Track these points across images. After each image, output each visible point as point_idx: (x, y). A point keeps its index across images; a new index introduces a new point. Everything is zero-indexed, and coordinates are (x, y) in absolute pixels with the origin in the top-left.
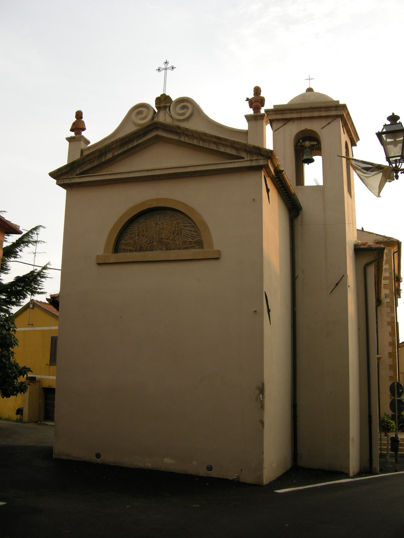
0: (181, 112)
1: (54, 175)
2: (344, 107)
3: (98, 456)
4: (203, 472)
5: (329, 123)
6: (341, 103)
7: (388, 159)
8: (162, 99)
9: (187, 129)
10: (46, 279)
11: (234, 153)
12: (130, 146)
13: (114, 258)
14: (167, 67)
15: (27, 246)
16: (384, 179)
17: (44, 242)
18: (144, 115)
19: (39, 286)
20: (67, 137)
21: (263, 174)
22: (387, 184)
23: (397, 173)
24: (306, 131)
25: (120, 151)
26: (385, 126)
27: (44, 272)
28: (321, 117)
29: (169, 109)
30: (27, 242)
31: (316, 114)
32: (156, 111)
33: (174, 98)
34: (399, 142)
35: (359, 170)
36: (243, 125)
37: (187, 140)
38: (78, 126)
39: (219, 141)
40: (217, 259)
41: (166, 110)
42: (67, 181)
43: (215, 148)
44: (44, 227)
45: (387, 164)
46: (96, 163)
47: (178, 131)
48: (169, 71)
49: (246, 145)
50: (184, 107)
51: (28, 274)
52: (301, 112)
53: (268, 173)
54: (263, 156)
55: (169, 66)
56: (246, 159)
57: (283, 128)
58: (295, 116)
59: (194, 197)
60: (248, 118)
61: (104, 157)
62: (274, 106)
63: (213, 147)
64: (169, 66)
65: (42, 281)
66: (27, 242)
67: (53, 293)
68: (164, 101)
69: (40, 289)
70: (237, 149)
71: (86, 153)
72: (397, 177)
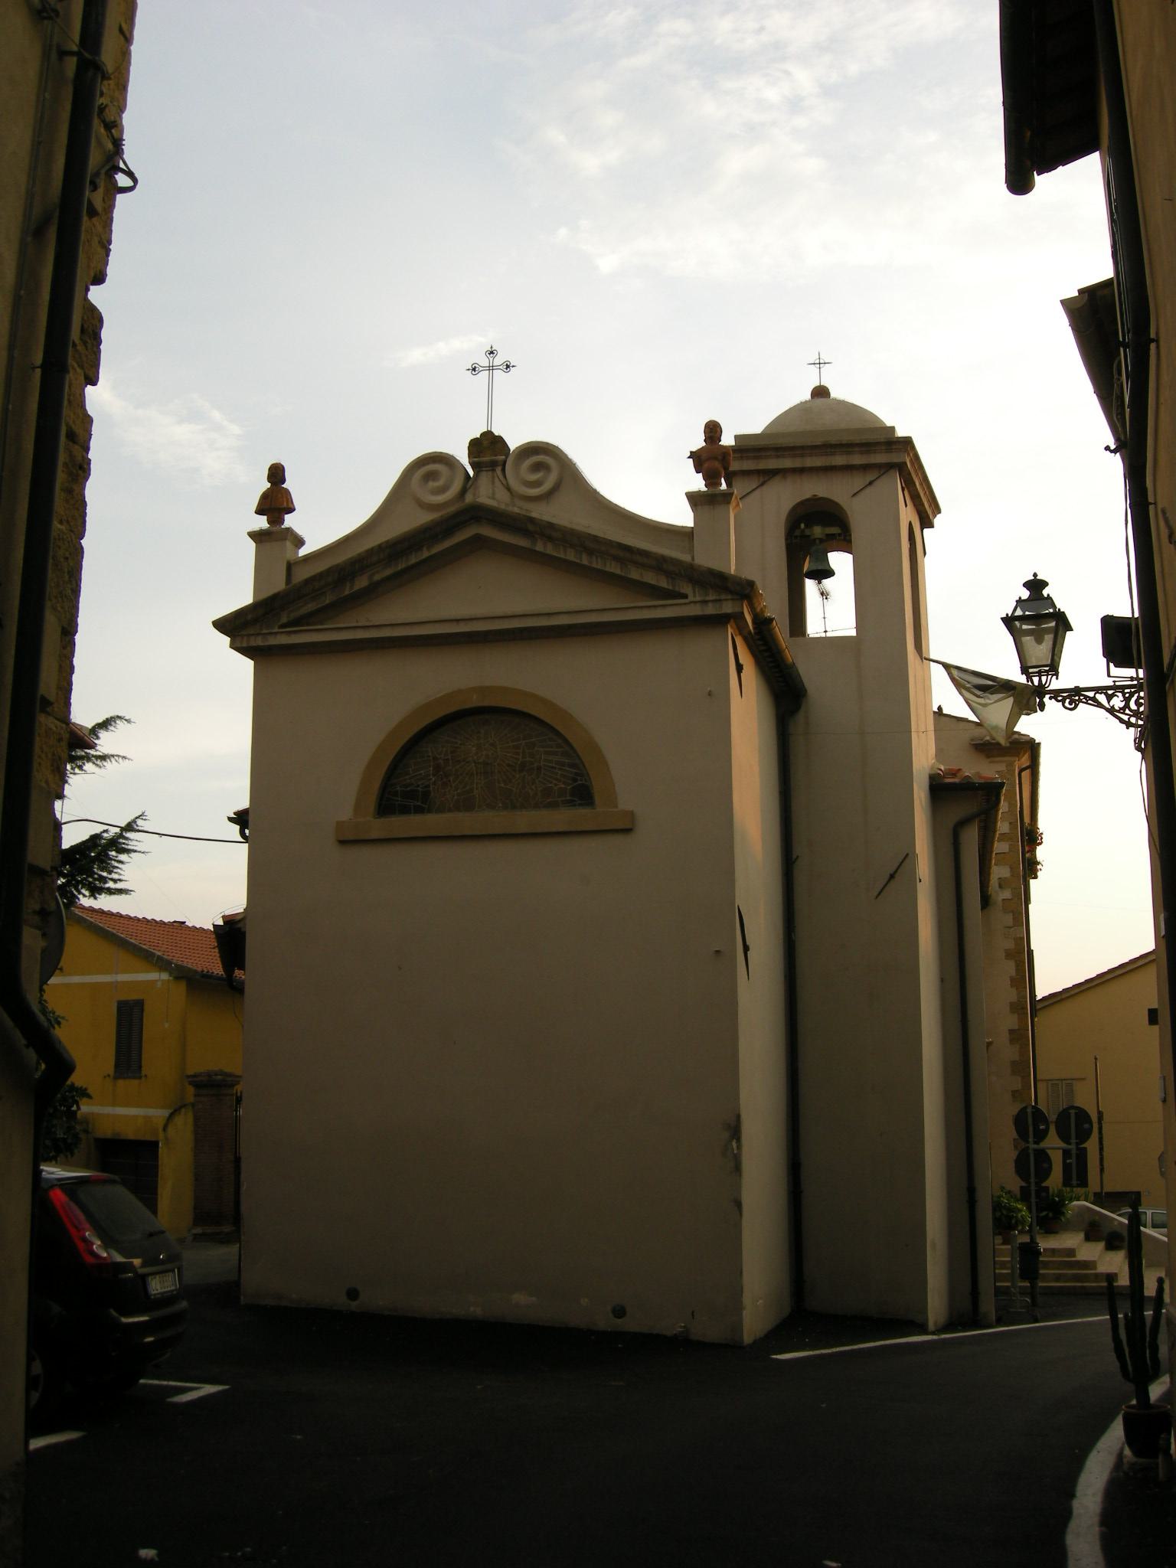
0: (534, 477)
1: (222, 625)
2: (907, 443)
3: (353, 1294)
4: (604, 1321)
5: (870, 483)
6: (901, 433)
7: (1025, 670)
8: (485, 443)
9: (551, 525)
10: (133, 855)
11: (664, 583)
12: (413, 559)
13: (380, 827)
14: (492, 364)
15: (80, 768)
16: (1016, 710)
17: (124, 758)
18: (440, 483)
19: (110, 872)
20: (250, 529)
21: (730, 630)
22: (1023, 717)
23: (1042, 697)
24: (815, 500)
25: (388, 572)
26: (1020, 602)
27: (127, 839)
28: (849, 468)
29: (503, 470)
30: (81, 758)
31: (839, 460)
32: (471, 473)
33: (513, 444)
34: (1047, 631)
35: (968, 690)
36: (683, 517)
37: (550, 550)
38: (275, 502)
39: (627, 554)
40: (627, 831)
41: (494, 470)
42: (259, 642)
43: (618, 571)
44: (128, 721)
45: (1022, 679)
46: (328, 599)
47: (531, 527)
48: (498, 374)
49: (691, 567)
50: (538, 467)
51: (84, 843)
52: (802, 456)
53: (741, 628)
54: (731, 592)
55: (498, 361)
56: (691, 598)
57: (757, 492)
58: (787, 463)
59: (575, 686)
60: (693, 498)
61: (348, 584)
62: (736, 437)
63: (613, 568)
64: (498, 361)
65: (122, 862)
66: (81, 758)
67: (227, 913)
68: (487, 447)
69: (115, 881)
70: (669, 574)
71: (302, 575)
72: (1042, 707)
